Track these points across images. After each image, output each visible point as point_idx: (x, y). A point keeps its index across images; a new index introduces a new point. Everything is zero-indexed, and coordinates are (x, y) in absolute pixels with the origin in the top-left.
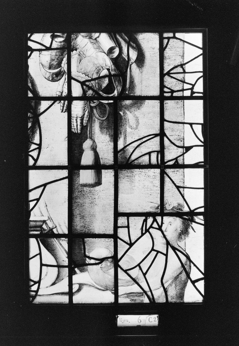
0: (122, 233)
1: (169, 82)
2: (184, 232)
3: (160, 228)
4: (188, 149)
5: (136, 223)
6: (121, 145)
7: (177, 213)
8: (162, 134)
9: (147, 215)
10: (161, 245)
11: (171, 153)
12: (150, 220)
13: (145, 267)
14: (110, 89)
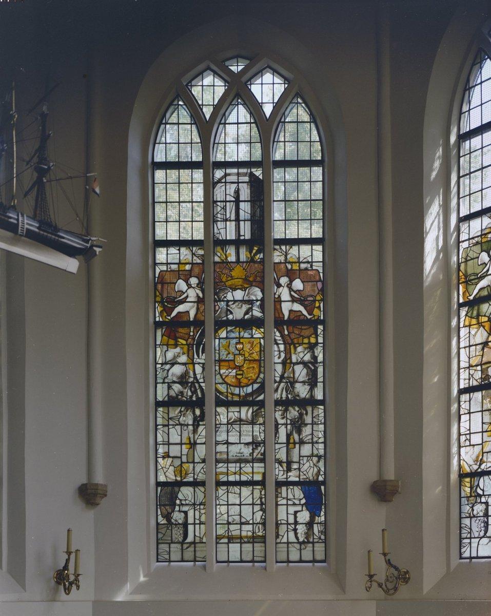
0: (301, 462)
1: (315, 420)
2: (318, 461)
3: (312, 460)
4: (320, 438)
5: (305, 459)
6: (301, 437)
7: (316, 456)
8: (312, 434)
9: (308, 456)
10: (312, 465)
11: (315, 439)
12: (309, 458)
13: (308, 471)
14: (298, 421)
